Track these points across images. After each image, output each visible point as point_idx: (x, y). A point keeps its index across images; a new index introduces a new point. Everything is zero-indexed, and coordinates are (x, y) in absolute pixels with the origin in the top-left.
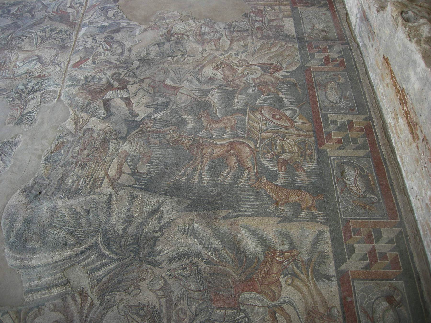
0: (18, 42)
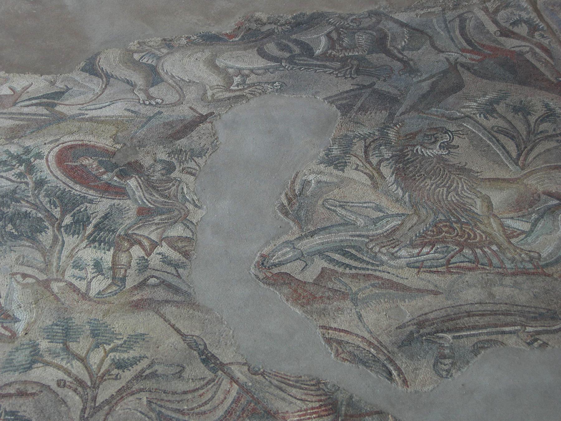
0: (436, 151)
